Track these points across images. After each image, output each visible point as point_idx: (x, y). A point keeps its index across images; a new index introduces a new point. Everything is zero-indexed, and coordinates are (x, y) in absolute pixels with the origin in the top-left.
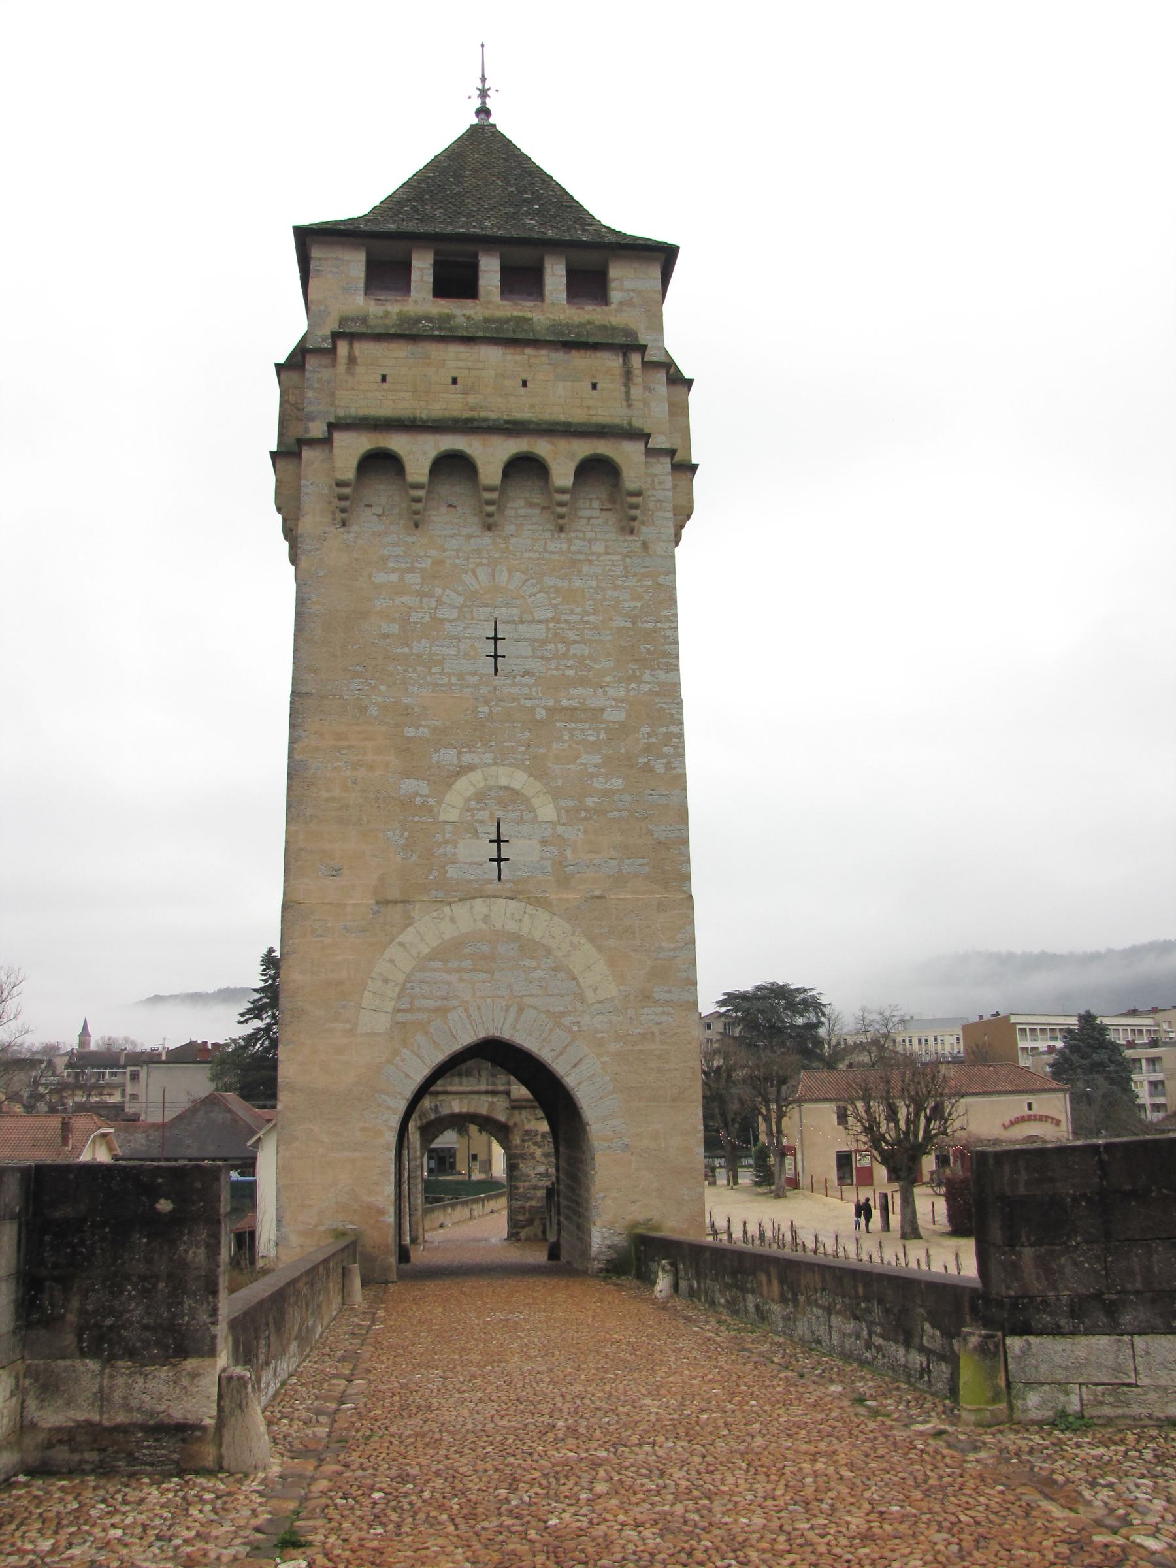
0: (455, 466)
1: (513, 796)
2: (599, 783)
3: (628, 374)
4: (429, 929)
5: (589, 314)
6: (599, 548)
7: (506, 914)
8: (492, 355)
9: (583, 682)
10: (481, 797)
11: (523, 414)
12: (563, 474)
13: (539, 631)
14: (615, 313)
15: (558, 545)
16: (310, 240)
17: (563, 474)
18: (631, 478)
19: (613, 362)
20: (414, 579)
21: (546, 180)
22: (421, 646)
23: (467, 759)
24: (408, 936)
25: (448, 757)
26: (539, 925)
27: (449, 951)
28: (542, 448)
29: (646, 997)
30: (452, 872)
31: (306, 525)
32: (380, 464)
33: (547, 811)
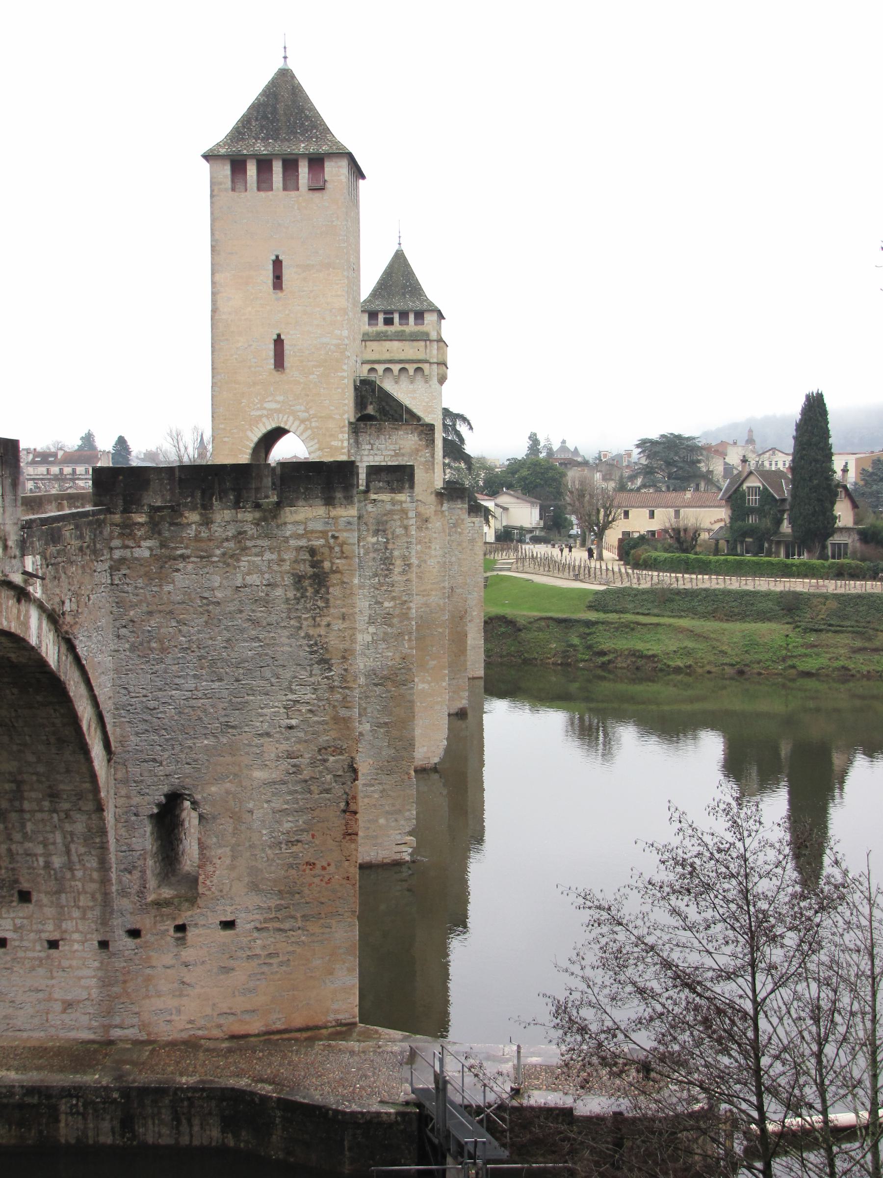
3: (426, 346)
17: (411, 372)
18: (426, 372)
28: (407, 366)
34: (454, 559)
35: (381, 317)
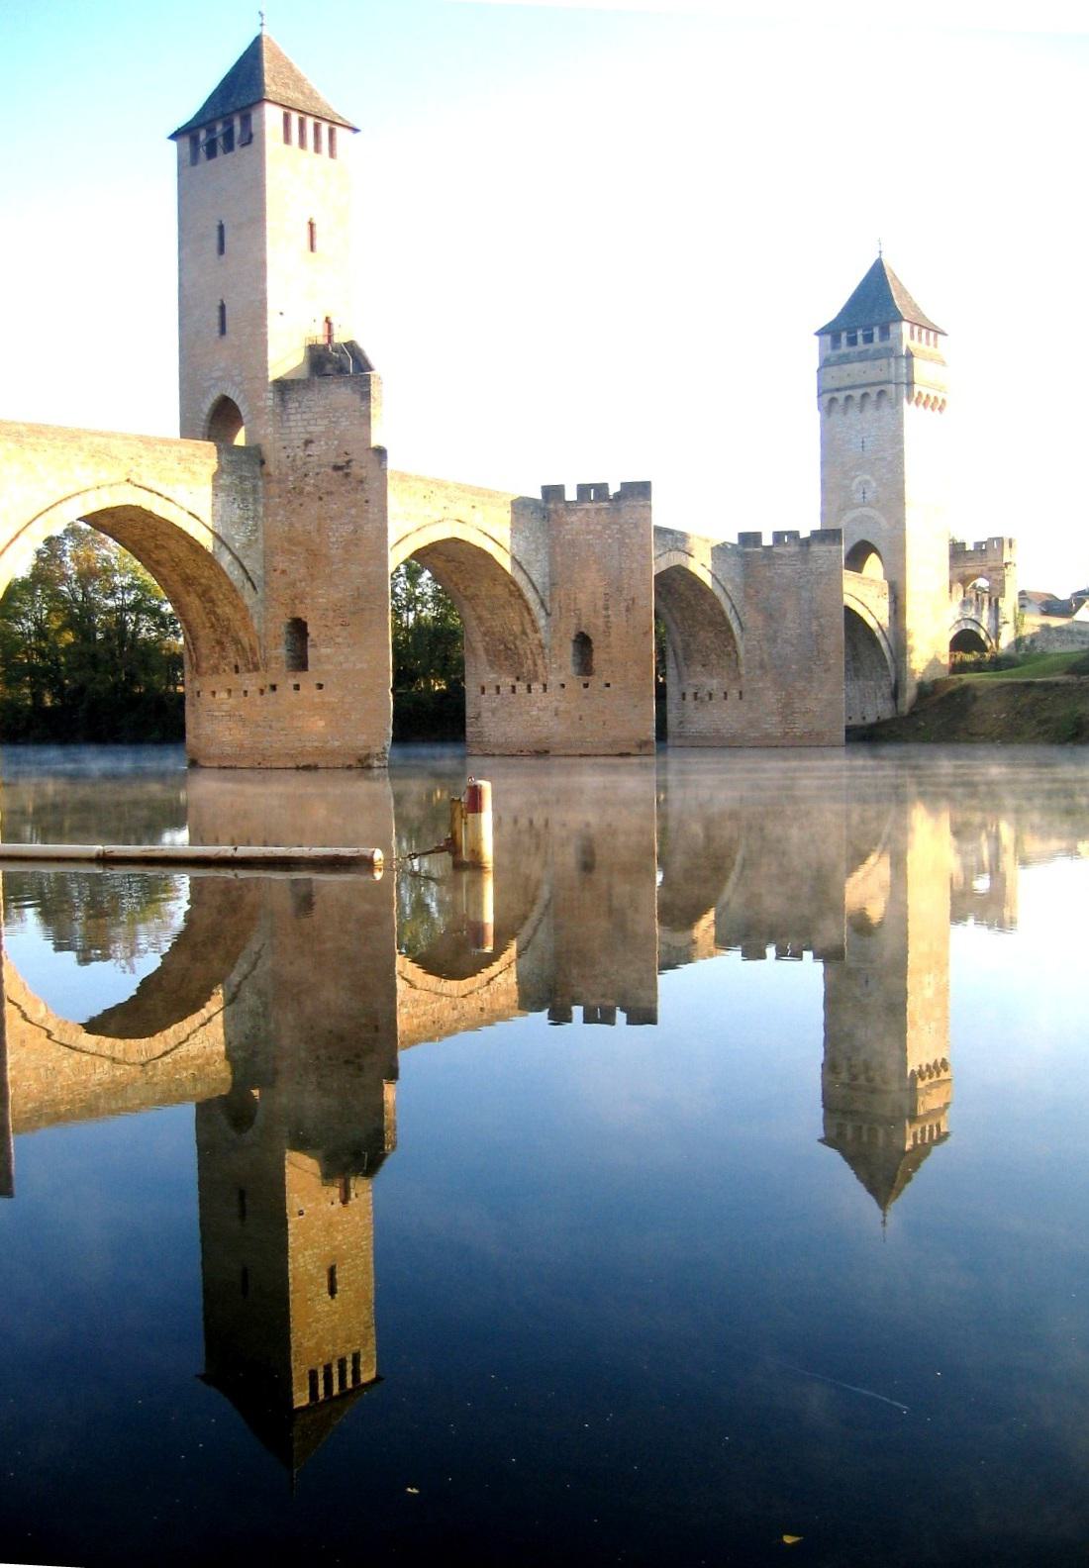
1: (867, 482)
7: (865, 510)
10: (860, 483)
11: (864, 382)
15: (876, 414)
23: (858, 473)
25: (853, 473)
26: (872, 512)
34: (635, 565)
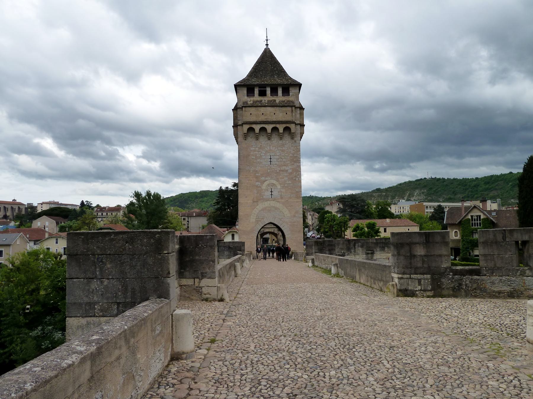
0: (263, 129)
1: (273, 185)
2: (287, 182)
3: (292, 111)
4: (261, 206)
5: (285, 98)
6: (287, 142)
7: (272, 203)
8: (269, 109)
9: (285, 165)
10: (268, 185)
11: (275, 120)
12: (281, 130)
13: (278, 157)
14: (291, 98)
15: (281, 142)
16: (236, 86)
17: (281, 130)
18: (293, 130)
19: (290, 109)
20: (257, 149)
21: (279, 64)
22: (259, 160)
23: (266, 179)
24: (258, 207)
25: (263, 178)
26: (278, 205)
27: (263, 209)
28: (278, 126)
29: (294, 216)
30: (264, 197)
31: (239, 140)
32: (251, 130)
33: (279, 187)
35: (256, 91)
